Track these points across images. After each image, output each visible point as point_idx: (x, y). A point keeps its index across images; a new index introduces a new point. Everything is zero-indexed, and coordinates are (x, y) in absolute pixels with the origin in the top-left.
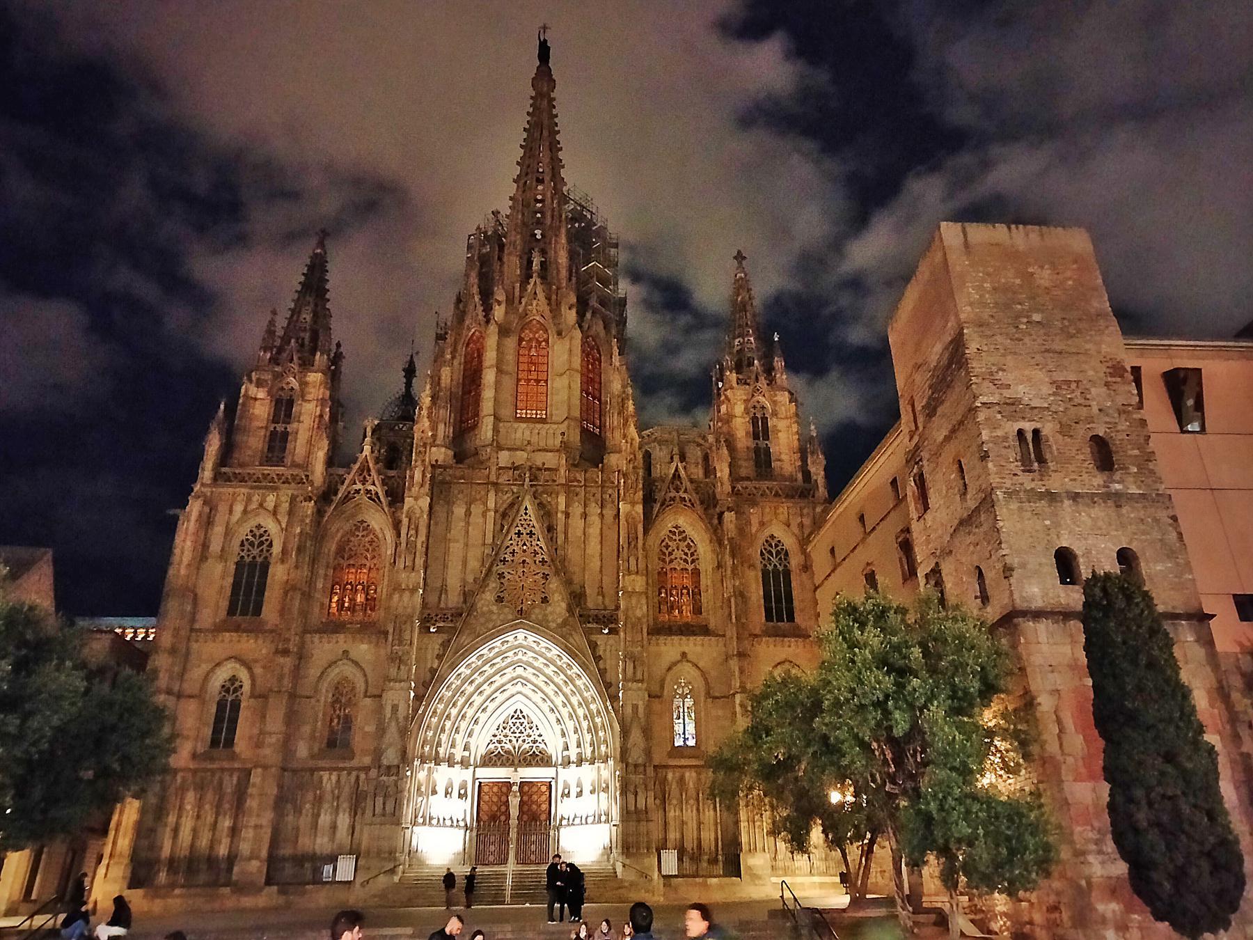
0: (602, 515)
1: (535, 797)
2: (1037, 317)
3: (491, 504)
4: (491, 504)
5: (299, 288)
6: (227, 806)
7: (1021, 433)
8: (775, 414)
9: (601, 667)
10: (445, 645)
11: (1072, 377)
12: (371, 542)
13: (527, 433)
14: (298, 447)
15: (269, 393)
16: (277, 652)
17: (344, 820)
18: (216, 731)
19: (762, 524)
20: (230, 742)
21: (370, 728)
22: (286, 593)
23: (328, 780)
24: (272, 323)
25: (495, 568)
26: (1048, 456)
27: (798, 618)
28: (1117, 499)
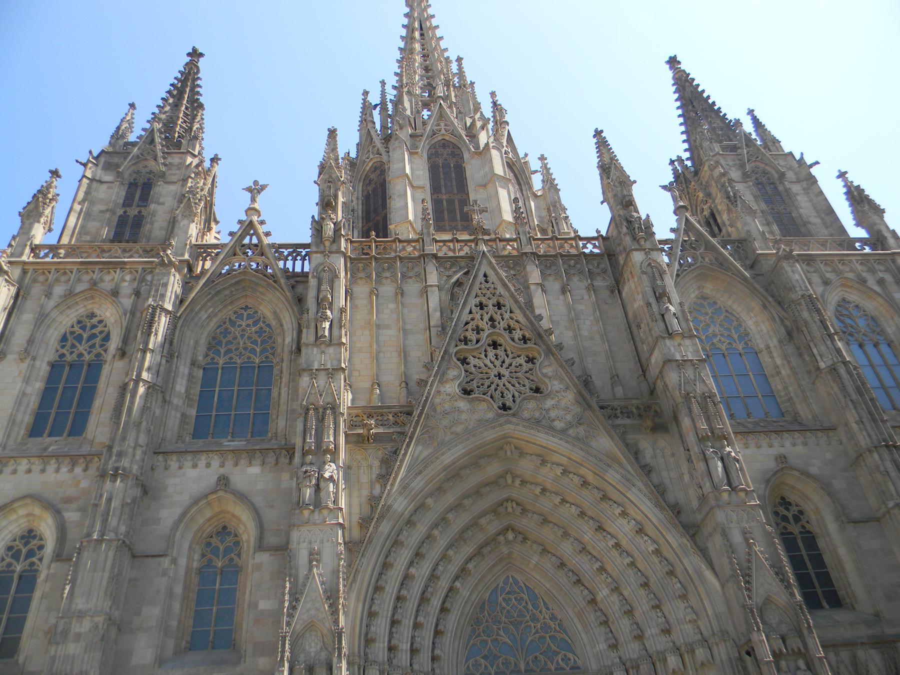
0: (591, 288)
4: (433, 278)
8: (782, 175)
9: (656, 481)
12: (260, 332)
14: (156, 226)
15: (119, 175)
25: (453, 350)
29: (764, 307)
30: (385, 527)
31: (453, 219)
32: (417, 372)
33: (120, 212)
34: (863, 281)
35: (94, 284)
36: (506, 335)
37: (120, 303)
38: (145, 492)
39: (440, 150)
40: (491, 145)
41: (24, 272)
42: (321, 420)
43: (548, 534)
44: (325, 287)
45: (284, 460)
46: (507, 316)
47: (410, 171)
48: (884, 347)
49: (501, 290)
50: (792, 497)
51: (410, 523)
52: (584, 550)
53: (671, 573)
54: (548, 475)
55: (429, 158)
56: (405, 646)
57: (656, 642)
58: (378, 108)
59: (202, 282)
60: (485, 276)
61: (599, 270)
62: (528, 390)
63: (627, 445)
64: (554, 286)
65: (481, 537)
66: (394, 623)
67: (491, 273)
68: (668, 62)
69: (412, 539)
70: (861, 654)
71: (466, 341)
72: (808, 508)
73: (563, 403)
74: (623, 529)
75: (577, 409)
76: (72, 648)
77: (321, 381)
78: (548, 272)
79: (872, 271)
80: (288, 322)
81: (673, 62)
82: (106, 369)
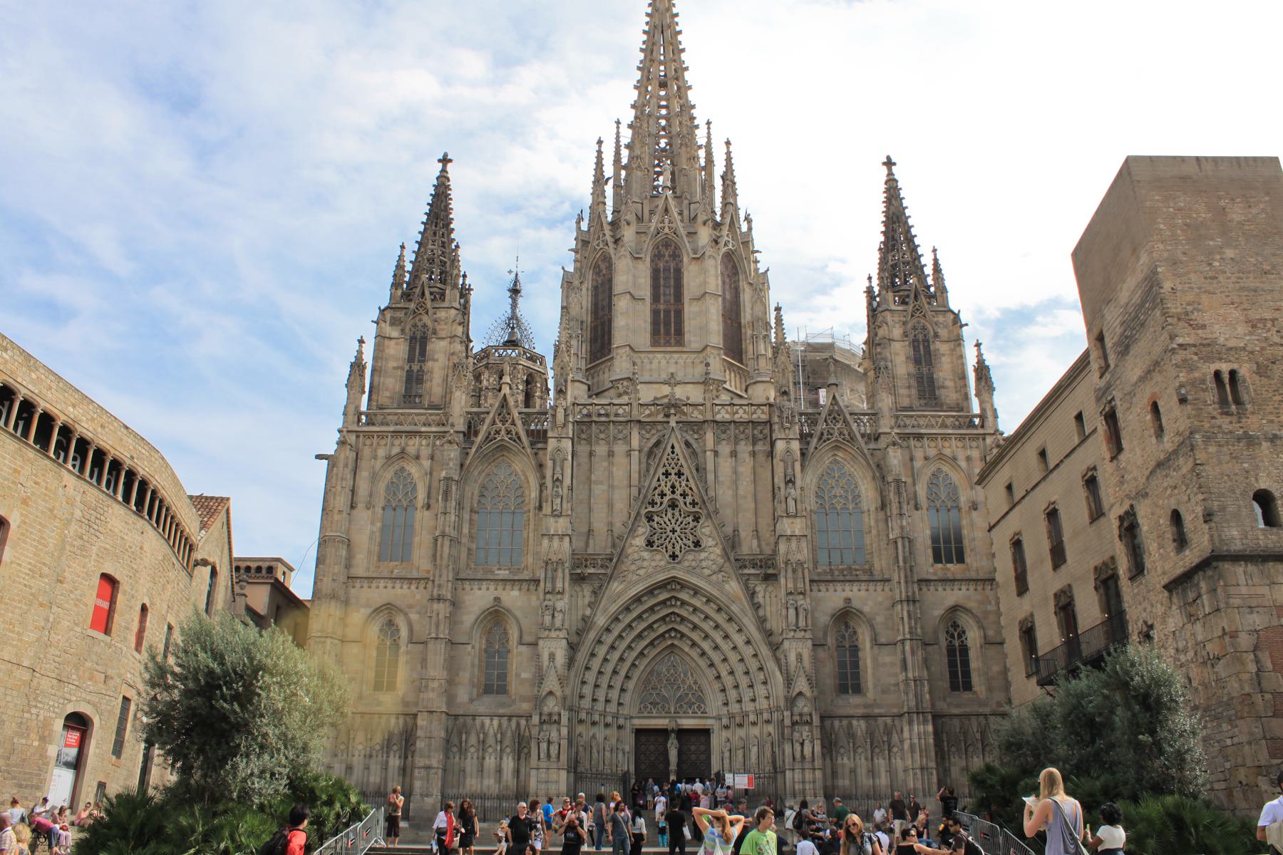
0: (754, 454)
1: (693, 748)
2: (1230, 253)
3: (635, 443)
4: (635, 443)
5: (425, 218)
6: (395, 748)
7: (1217, 374)
8: (936, 335)
10: (594, 593)
13: (664, 362)
14: (434, 386)
15: (403, 330)
17: (509, 764)
18: (379, 675)
19: (926, 458)
22: (436, 540)
23: (492, 725)
24: (401, 257)
26: (1245, 398)
27: (968, 559)
29: (874, 478)
30: (592, 635)
31: (667, 333)
32: (618, 528)
33: (407, 368)
34: (955, 459)
36: (681, 499)
37: (421, 465)
38: (453, 604)
39: (663, 250)
40: (707, 254)
41: (358, 437)
42: (556, 570)
43: (696, 636)
44: (558, 469)
45: (532, 587)
46: (683, 484)
47: (632, 278)
48: (954, 512)
49: (682, 461)
50: (851, 624)
51: (608, 630)
52: (717, 648)
55: (652, 261)
56: (602, 699)
57: (749, 707)
58: (611, 183)
59: (474, 450)
60: (673, 447)
61: (761, 436)
62: (692, 546)
63: (747, 588)
64: (725, 449)
66: (596, 686)
67: (676, 445)
68: (884, 164)
69: (609, 639)
70: (855, 722)
71: (653, 503)
72: (860, 631)
73: (712, 557)
74: (739, 639)
76: (431, 695)
77: (556, 542)
78: (724, 436)
81: (889, 163)
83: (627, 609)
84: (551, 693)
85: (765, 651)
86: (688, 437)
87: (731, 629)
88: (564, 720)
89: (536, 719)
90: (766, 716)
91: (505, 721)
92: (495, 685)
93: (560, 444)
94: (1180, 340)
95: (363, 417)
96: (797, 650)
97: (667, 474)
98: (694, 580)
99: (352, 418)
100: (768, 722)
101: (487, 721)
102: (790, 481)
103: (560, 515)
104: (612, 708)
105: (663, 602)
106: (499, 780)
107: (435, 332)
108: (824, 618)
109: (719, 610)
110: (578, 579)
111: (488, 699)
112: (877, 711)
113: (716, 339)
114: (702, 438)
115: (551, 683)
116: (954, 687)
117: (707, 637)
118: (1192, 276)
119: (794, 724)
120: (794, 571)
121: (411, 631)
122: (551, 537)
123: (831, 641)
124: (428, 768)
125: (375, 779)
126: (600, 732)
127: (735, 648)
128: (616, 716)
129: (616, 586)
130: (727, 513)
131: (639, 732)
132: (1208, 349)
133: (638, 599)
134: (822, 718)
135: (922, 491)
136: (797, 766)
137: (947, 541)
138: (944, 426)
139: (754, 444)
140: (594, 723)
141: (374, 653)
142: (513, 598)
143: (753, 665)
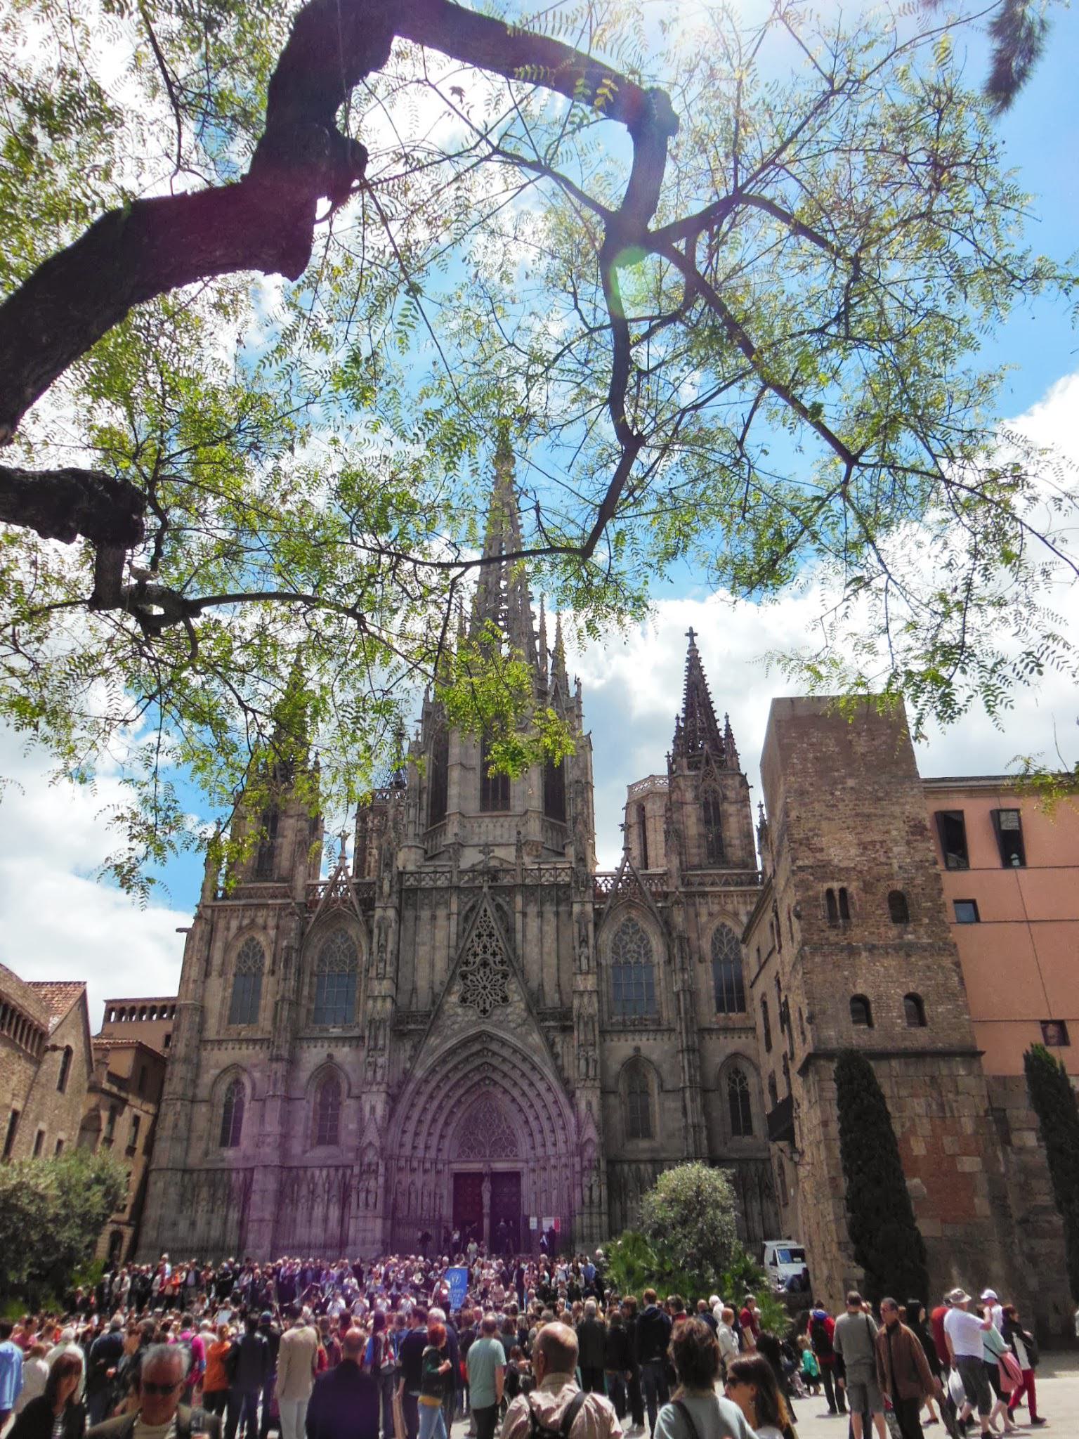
0: (557, 914)
2: (851, 783)
4: (454, 908)
7: (830, 892)
8: (725, 798)
10: (415, 1048)
11: (877, 837)
12: (349, 947)
16: (271, 1060)
17: (334, 1213)
18: (225, 1131)
19: (710, 914)
20: (236, 1142)
21: (352, 1126)
23: (320, 1176)
26: (851, 912)
28: (907, 950)
31: (495, 797)
34: (736, 914)
35: (253, 921)
43: (507, 1084)
51: (426, 1081)
52: (524, 1094)
53: (560, 1115)
54: (506, 1053)
56: (422, 1146)
57: (551, 1150)
63: (547, 1039)
64: (532, 909)
65: (469, 1083)
66: (416, 1134)
71: (467, 963)
74: (541, 1087)
75: (525, 1015)
76: (268, 1150)
77: (379, 1003)
79: (745, 903)
80: (365, 948)
82: (265, 980)
83: (443, 1061)
84: (370, 1144)
85: (562, 1098)
86: (500, 900)
87: (535, 1078)
88: (382, 1169)
89: (356, 1170)
90: (563, 1160)
91: (332, 1171)
92: (326, 1133)
93: (385, 912)
94: (800, 863)
95: (220, 894)
96: (588, 1098)
97: (479, 936)
98: (501, 1034)
99: (208, 893)
100: (566, 1166)
101: (317, 1173)
102: (584, 941)
103: (384, 978)
104: (432, 1154)
105: (477, 1053)
106: (325, 1230)
107: (285, 812)
108: (615, 1066)
109: (524, 1059)
110: (399, 1034)
111: (321, 1152)
112: (663, 1155)
113: (536, 803)
114: (511, 902)
115: (372, 1136)
116: (736, 1131)
117: (515, 1084)
118: (816, 805)
119: (583, 1169)
120: (586, 1024)
121: (254, 1088)
122: (375, 998)
123: (622, 1088)
124: (261, 1220)
125: (215, 1233)
126: (419, 1179)
127: (539, 1095)
128: (435, 1162)
129: (433, 1041)
130: (533, 969)
131: (458, 1177)
132: (823, 870)
133: (452, 1052)
134: (611, 1163)
135: (706, 945)
136: (586, 1210)
137: (729, 990)
138: (727, 883)
139: (558, 904)
140: (413, 1170)
141: (222, 1111)
142: (344, 1054)
143: (554, 1111)
